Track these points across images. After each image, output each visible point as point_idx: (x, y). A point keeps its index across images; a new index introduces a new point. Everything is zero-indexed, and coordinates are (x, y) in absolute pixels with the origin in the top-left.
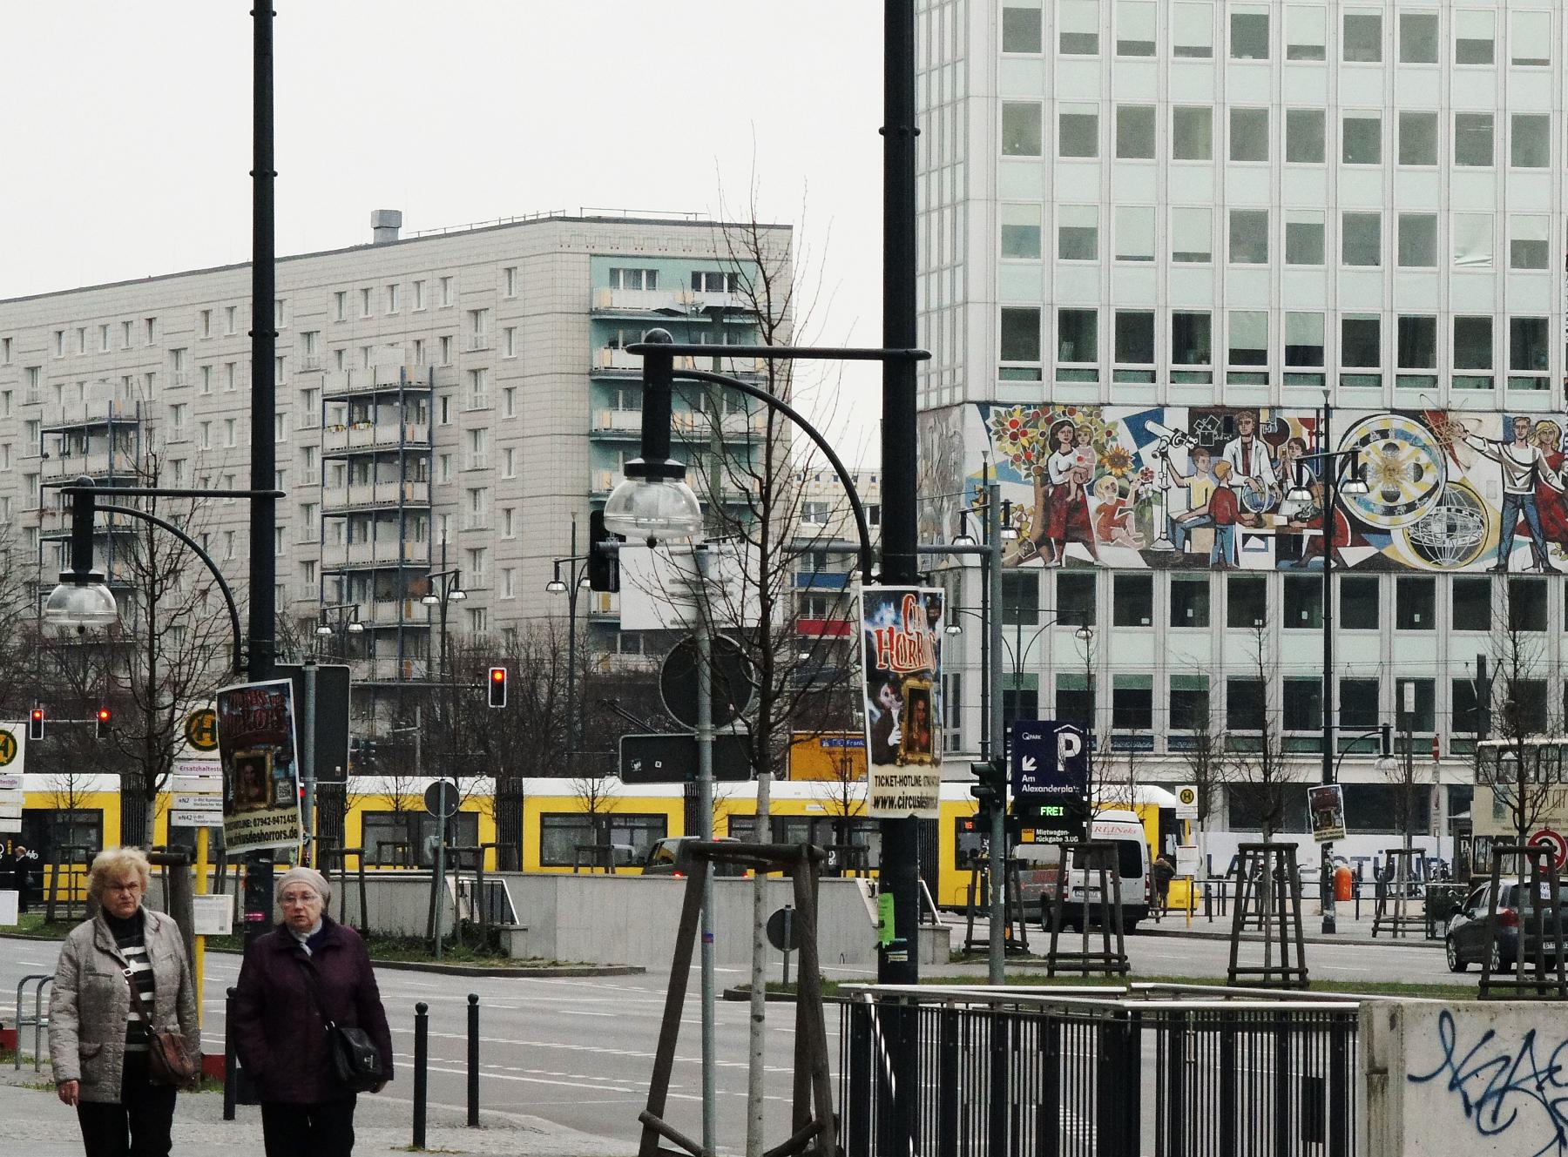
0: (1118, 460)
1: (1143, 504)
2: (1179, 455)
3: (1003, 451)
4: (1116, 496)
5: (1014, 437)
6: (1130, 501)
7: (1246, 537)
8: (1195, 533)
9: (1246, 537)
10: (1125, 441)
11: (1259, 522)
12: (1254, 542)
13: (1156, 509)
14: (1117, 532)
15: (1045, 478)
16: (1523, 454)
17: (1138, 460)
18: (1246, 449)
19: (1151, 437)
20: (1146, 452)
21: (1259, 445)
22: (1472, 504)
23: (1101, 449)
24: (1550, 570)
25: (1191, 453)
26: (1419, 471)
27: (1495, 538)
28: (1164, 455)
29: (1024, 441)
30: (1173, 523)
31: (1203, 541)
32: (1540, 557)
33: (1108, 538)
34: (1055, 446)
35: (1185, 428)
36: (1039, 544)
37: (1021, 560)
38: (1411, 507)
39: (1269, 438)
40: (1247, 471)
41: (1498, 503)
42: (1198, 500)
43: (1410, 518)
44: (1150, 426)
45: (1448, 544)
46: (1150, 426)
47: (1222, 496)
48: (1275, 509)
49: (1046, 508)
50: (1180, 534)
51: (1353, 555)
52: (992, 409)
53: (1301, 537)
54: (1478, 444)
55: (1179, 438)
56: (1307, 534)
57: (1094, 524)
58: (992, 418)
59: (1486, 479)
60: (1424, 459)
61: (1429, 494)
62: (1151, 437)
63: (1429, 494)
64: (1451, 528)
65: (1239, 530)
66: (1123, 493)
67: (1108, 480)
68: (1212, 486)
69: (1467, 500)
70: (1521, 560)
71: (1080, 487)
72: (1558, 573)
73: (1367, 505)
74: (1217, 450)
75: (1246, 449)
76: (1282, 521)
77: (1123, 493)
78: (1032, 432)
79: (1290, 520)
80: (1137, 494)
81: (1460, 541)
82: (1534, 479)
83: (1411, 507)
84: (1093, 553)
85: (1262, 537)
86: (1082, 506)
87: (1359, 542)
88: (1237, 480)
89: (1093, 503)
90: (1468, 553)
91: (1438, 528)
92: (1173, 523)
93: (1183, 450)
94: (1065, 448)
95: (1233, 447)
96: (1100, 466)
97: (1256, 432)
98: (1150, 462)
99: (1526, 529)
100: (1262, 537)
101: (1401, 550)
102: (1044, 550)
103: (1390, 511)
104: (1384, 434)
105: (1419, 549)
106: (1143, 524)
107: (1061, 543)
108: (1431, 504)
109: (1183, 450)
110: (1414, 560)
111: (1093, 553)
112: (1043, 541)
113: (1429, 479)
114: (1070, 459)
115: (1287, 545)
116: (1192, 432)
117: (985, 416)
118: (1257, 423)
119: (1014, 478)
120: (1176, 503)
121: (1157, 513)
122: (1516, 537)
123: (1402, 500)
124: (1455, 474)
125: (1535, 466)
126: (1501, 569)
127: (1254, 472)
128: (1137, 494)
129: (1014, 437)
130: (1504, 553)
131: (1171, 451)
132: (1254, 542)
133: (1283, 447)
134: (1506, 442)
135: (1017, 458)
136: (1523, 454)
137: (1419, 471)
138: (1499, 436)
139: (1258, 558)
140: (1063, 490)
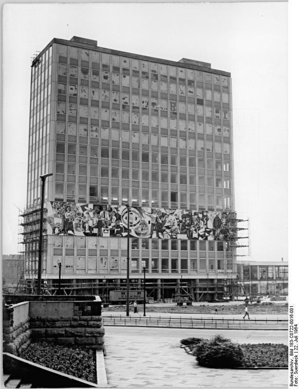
0: (79, 214)
1: (84, 223)
2: (91, 214)
4: (78, 221)
5: (58, 209)
6: (81, 223)
7: (104, 230)
8: (94, 229)
9: (104, 230)
10: (81, 211)
11: (107, 227)
12: (106, 231)
13: (86, 224)
14: (78, 228)
15: (64, 216)
16: (155, 216)
17: (83, 215)
18: (104, 213)
19: (86, 210)
20: (85, 213)
21: (107, 212)
22: (146, 225)
23: (75, 212)
24: (159, 238)
25: (93, 213)
26: (136, 219)
27: (150, 232)
28: (88, 214)
29: (60, 209)
30: (90, 227)
31: (95, 231)
32: (158, 235)
33: (77, 230)
34: (66, 211)
35: (92, 208)
36: (63, 231)
37: (59, 234)
38: (135, 225)
39: (109, 211)
40: (104, 217)
42: (95, 223)
43: (135, 227)
44: (86, 208)
45: (142, 232)
46: (86, 208)
47: (100, 222)
49: (64, 223)
50: (91, 229)
52: (53, 203)
53: (114, 231)
54: (147, 213)
55: (91, 210)
56: (116, 230)
57: (74, 226)
58: (54, 204)
59: (147, 219)
60: (137, 216)
61: (138, 223)
62: (86, 210)
63: (138, 223)
64: (142, 229)
65: (103, 229)
66: (80, 221)
67: (77, 218)
68: (98, 220)
69: (144, 224)
71: (71, 219)
72: (161, 238)
74: (99, 213)
75: (104, 213)
76: (111, 227)
77: (80, 221)
78: (62, 208)
79: (113, 227)
80: (83, 221)
81: (144, 232)
82: (156, 221)
83: (135, 225)
84: (73, 232)
85: (107, 230)
86: (71, 223)
87: (125, 232)
88: (103, 219)
91: (140, 229)
92: (90, 227)
93: (92, 212)
94: (68, 211)
95: (102, 212)
96: (75, 215)
97: (106, 209)
98: (85, 215)
99: (155, 230)
100: (107, 230)
101: (133, 233)
102: (64, 232)
105: (136, 233)
106: (84, 228)
107: (67, 230)
108: (138, 225)
109: (92, 212)
111: (73, 232)
113: (138, 220)
114: (68, 214)
116: (94, 209)
117: (52, 204)
118: (106, 208)
120: (91, 224)
121: (87, 225)
122: (154, 232)
123: (133, 224)
124: (143, 219)
125: (157, 218)
126: (151, 237)
127: (106, 217)
128: (83, 221)
129: (58, 209)
131: (90, 213)
132: (106, 231)
133: (111, 213)
134: (152, 213)
135: (58, 213)
136: (155, 216)
137: (136, 219)
138: (150, 212)
140: (68, 220)
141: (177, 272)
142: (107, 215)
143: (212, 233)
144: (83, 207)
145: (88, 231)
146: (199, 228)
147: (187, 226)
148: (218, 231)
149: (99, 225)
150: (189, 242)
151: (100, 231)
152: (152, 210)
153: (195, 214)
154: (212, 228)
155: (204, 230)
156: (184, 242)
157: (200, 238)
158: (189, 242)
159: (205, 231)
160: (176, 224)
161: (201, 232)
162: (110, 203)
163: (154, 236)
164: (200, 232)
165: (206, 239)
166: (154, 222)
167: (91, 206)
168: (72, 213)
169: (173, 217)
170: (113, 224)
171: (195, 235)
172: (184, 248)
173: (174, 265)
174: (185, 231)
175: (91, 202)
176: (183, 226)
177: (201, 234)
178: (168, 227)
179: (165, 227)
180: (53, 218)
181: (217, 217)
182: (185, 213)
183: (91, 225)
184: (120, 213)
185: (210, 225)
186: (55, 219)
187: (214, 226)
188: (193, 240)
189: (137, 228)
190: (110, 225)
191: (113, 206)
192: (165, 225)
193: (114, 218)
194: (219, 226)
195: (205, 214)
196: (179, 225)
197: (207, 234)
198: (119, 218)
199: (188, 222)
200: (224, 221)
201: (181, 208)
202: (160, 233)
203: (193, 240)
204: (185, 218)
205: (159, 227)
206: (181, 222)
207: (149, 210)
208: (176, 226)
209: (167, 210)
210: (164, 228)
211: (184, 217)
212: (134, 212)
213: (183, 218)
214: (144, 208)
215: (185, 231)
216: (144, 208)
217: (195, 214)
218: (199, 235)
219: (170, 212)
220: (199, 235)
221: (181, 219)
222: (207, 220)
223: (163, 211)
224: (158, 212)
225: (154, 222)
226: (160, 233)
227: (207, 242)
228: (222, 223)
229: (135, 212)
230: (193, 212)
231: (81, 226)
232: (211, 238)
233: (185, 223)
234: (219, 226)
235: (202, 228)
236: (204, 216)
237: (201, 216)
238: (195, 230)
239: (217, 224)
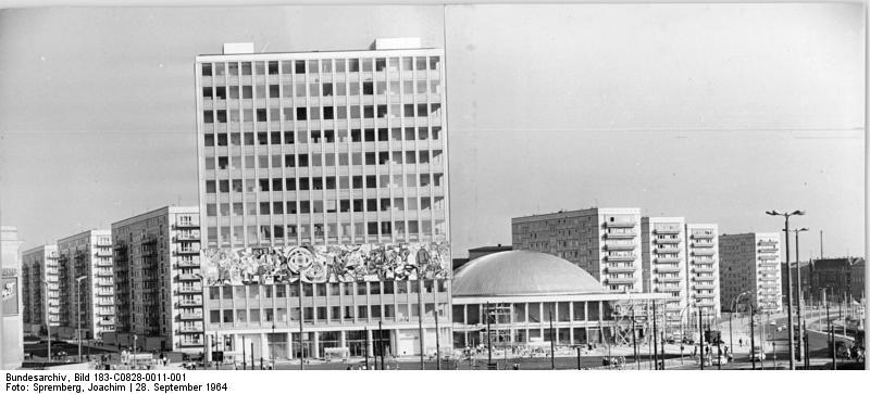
0: (235, 261)
1: (242, 271)
2: (250, 259)
3: (209, 260)
10: (237, 257)
16: (332, 255)
31: (256, 279)
32: (337, 279)
47: (260, 268)
51: (292, 280)
70: (332, 280)
74: (259, 257)
81: (318, 275)
89: (231, 271)
90: (320, 278)
91: (312, 273)
95: (263, 257)
101: (303, 279)
105: (308, 278)
110: (308, 281)
112: (219, 280)
115: (276, 278)
121: (245, 273)
130: (328, 279)
136: (332, 255)
139: (270, 281)
142: (269, 258)
143: (414, 270)
144: (239, 253)
145: (246, 280)
146: (396, 266)
148: (425, 267)
149: (260, 272)
150: (382, 284)
152: (328, 248)
153: (390, 248)
157: (397, 278)
158: (382, 284)
159: (405, 268)
160: (362, 262)
165: (407, 278)
166: (332, 263)
167: (249, 250)
168: (228, 260)
169: (358, 255)
170: (277, 270)
171: (390, 275)
175: (250, 246)
176: (371, 264)
178: (351, 268)
181: (422, 249)
182: (375, 247)
183: (250, 272)
184: (285, 255)
185: (412, 260)
191: (276, 249)
192: (348, 265)
193: (279, 262)
195: (404, 247)
196: (366, 264)
197: (407, 273)
198: (285, 261)
200: (434, 253)
201: (370, 242)
202: (340, 276)
205: (339, 268)
207: (324, 249)
208: (362, 265)
210: (345, 269)
211: (374, 253)
213: (371, 254)
214: (317, 247)
216: (317, 247)
217: (390, 248)
218: (395, 275)
220: (395, 275)
222: (407, 254)
223: (343, 247)
224: (335, 250)
225: (332, 263)
227: (408, 283)
228: (429, 257)
230: (386, 246)
232: (413, 276)
236: (402, 250)
237: (397, 250)
238: (390, 269)
239: (422, 259)
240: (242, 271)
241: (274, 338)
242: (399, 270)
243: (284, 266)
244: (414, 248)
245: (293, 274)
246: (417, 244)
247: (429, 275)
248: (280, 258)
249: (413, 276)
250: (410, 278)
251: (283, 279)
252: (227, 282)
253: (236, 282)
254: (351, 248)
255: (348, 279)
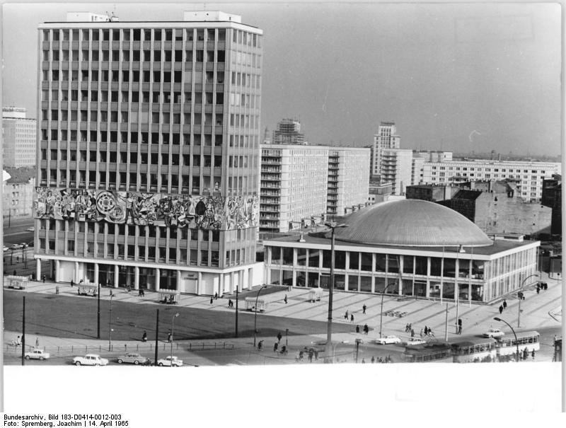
6: (60, 207)
15: (46, 202)
20: (63, 197)
24: (135, 224)
27: (125, 217)
30: (68, 211)
31: (73, 215)
32: (133, 222)
38: (110, 210)
41: (124, 208)
42: (72, 207)
46: (64, 192)
48: (86, 209)
51: (99, 219)
69: (119, 209)
73: (101, 209)
74: (75, 198)
82: (132, 206)
91: (114, 214)
95: (78, 197)
103: (106, 211)
104: (105, 195)
112: (46, 214)
119: (41, 201)
121: (65, 210)
123: (109, 208)
125: (132, 203)
126: (126, 223)
130: (126, 220)
136: (130, 200)
139: (83, 219)
141: (123, 258)
142: (83, 200)
144: (62, 192)
145: (66, 215)
146: (180, 214)
147: (166, 211)
148: (202, 218)
151: (76, 215)
152: (128, 194)
154: (194, 214)
155: (184, 216)
156: (162, 229)
157: (180, 226)
159: (186, 217)
161: (181, 219)
162: (87, 188)
163: (129, 221)
164: (179, 219)
165: (187, 225)
166: (130, 207)
168: (53, 198)
170: (88, 209)
171: (174, 222)
172: (163, 235)
173: (112, 251)
174: (162, 217)
177: (181, 221)
178: (144, 213)
179: (142, 212)
180: (37, 203)
183: (69, 210)
184: (95, 197)
185: (192, 212)
186: (39, 203)
187: (197, 212)
188: (173, 228)
189: (112, 213)
190: (86, 209)
192: (142, 211)
193: (90, 202)
194: (202, 213)
195: (186, 198)
196: (156, 211)
197: (187, 222)
198: (94, 201)
199: (167, 207)
201: (161, 191)
202: (135, 219)
203: (173, 228)
204: (164, 203)
206: (158, 207)
207: (124, 194)
208: (153, 211)
209: (144, 195)
210: (140, 214)
211: (163, 201)
212: (108, 196)
213: (161, 202)
214: (120, 193)
215: (162, 217)
219: (148, 196)
220: (178, 222)
221: (158, 204)
226: (135, 219)
228: (206, 209)
229: (110, 196)
231: (61, 210)
233: (163, 208)
234: (202, 213)
235: (183, 214)
238: (175, 217)
240: (63, 207)
241: (90, 267)
242: (181, 219)
243: (94, 207)
244: (194, 200)
245: (100, 213)
246: (198, 197)
247: (205, 225)
248: (91, 200)
249: (192, 225)
250: (190, 226)
251: (92, 217)
252: (51, 216)
253: (58, 215)
254: (145, 196)
255: (142, 222)
